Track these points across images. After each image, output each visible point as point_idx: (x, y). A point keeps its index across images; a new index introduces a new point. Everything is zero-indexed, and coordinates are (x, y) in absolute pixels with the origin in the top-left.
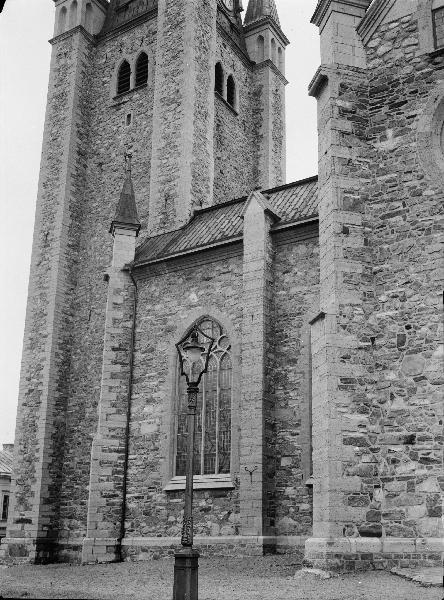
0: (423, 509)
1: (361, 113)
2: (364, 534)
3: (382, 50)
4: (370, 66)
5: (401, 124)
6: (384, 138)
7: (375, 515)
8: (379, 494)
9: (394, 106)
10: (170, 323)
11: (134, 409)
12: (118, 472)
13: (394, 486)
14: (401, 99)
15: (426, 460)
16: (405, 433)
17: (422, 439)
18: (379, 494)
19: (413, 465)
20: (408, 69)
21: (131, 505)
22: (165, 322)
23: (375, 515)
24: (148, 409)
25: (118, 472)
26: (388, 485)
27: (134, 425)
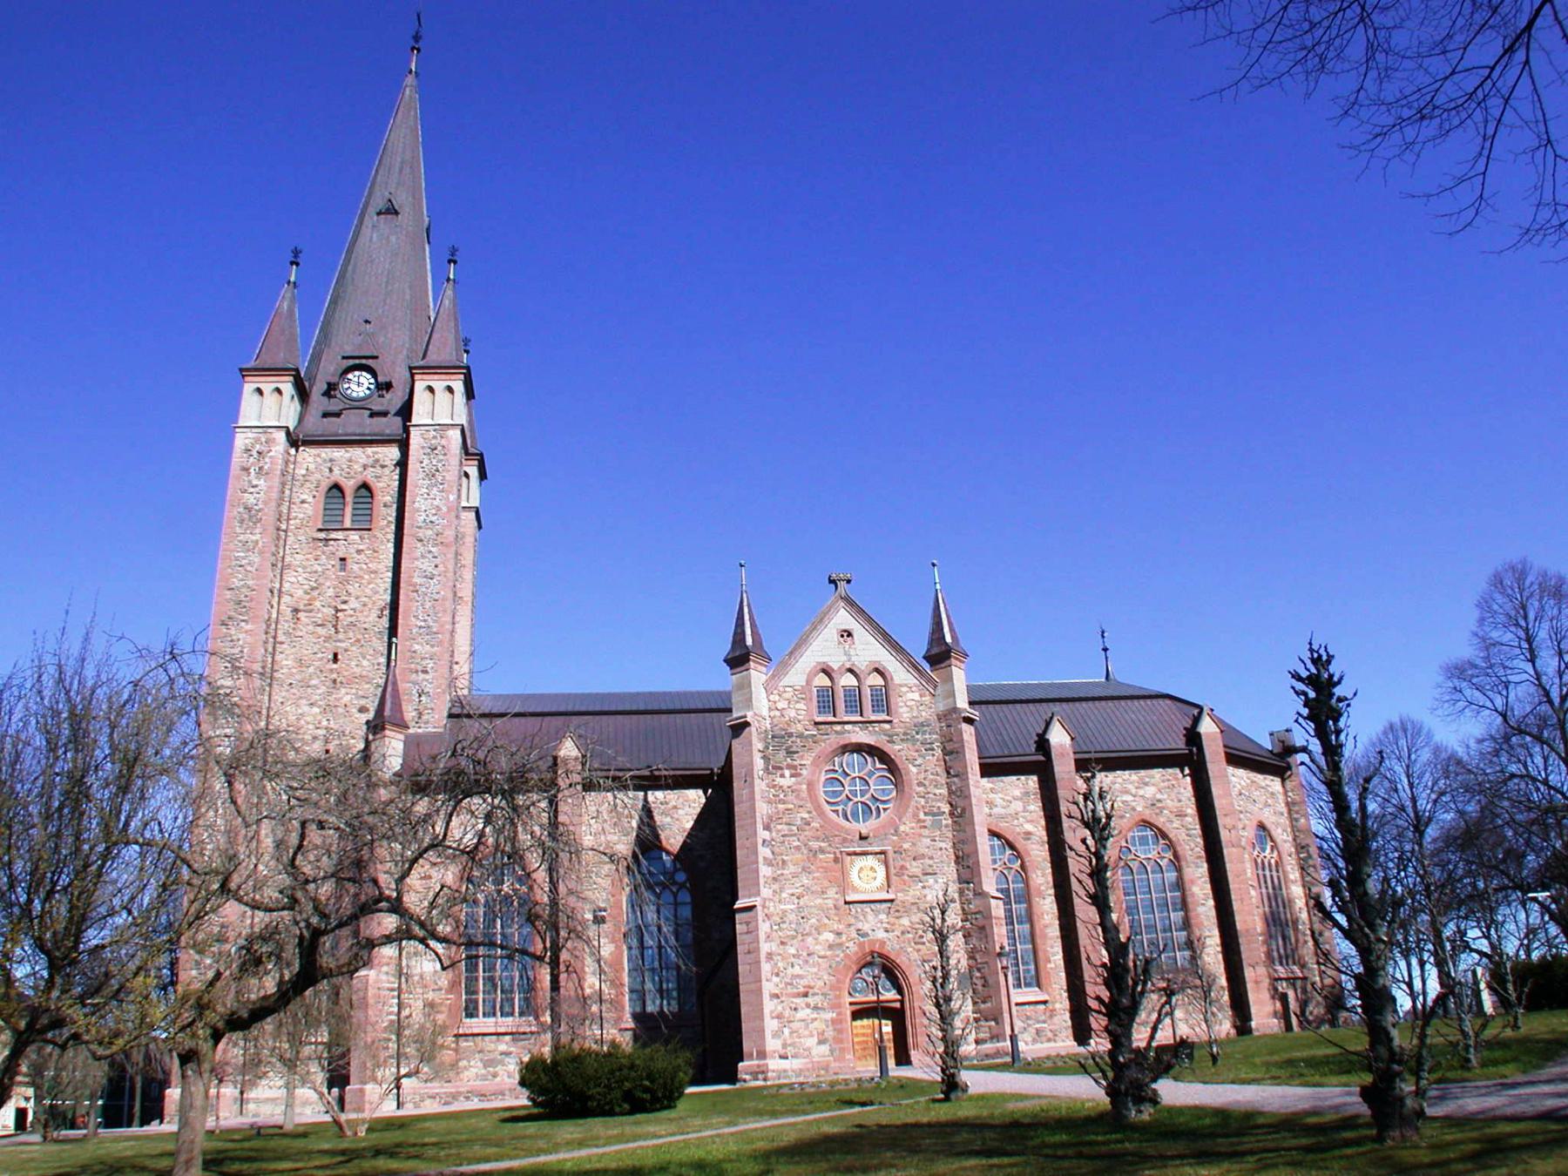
3: (780, 706)
4: (772, 714)
5: (795, 767)
6: (782, 776)
8: (786, 1031)
9: (790, 753)
13: (795, 1025)
14: (794, 749)
15: (816, 1008)
16: (802, 990)
17: (814, 995)
19: (808, 1011)
20: (800, 727)
25: (391, 1013)
26: (791, 1025)
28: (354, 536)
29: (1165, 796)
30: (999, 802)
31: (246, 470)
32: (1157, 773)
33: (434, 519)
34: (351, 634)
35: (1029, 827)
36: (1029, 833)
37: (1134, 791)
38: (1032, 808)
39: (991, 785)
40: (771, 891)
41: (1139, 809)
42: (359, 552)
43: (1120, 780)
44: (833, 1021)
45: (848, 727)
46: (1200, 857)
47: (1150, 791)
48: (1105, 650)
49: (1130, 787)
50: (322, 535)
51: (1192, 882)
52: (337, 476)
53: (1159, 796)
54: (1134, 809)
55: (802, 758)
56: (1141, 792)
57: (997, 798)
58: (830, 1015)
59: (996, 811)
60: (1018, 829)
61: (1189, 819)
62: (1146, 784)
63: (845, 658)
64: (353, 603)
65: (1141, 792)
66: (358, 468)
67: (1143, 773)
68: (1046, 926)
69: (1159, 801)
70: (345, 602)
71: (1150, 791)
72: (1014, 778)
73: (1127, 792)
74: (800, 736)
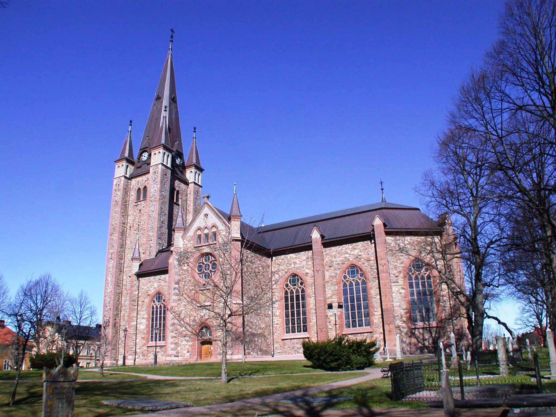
0: (186, 351)
1: (180, 259)
2: (175, 356)
7: (178, 353)
10: (149, 293)
11: (138, 320)
12: (134, 340)
13: (182, 346)
15: (187, 341)
18: (179, 348)
19: (185, 342)
21: (138, 351)
22: (147, 292)
23: (178, 353)
24: (143, 320)
25: (134, 340)
27: (138, 326)
28: (143, 203)
29: (363, 253)
30: (298, 262)
31: (116, 190)
32: (360, 244)
33: (154, 194)
34: (142, 232)
35: (307, 271)
36: (307, 273)
37: (349, 253)
38: (309, 263)
39: (295, 256)
40: (176, 304)
41: (351, 260)
42: (144, 207)
43: (344, 249)
44: (192, 345)
45: (203, 247)
46: (375, 278)
47: (356, 252)
48: (382, 189)
49: (348, 251)
50: (136, 204)
51: (371, 288)
52: (140, 186)
53: (360, 253)
54: (349, 260)
55: (190, 259)
56: (353, 252)
57: (297, 261)
58: (191, 343)
59: (296, 265)
60: (303, 272)
61: (372, 262)
62: (355, 249)
63: (205, 224)
64: (142, 223)
65: (353, 252)
66: (144, 182)
67: (354, 244)
68: (311, 309)
69: (360, 255)
70: (140, 223)
71: (356, 252)
72: (304, 252)
73: (347, 253)
74: (191, 252)
